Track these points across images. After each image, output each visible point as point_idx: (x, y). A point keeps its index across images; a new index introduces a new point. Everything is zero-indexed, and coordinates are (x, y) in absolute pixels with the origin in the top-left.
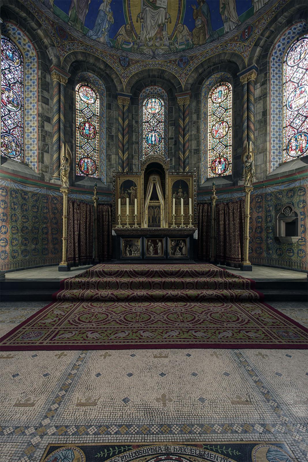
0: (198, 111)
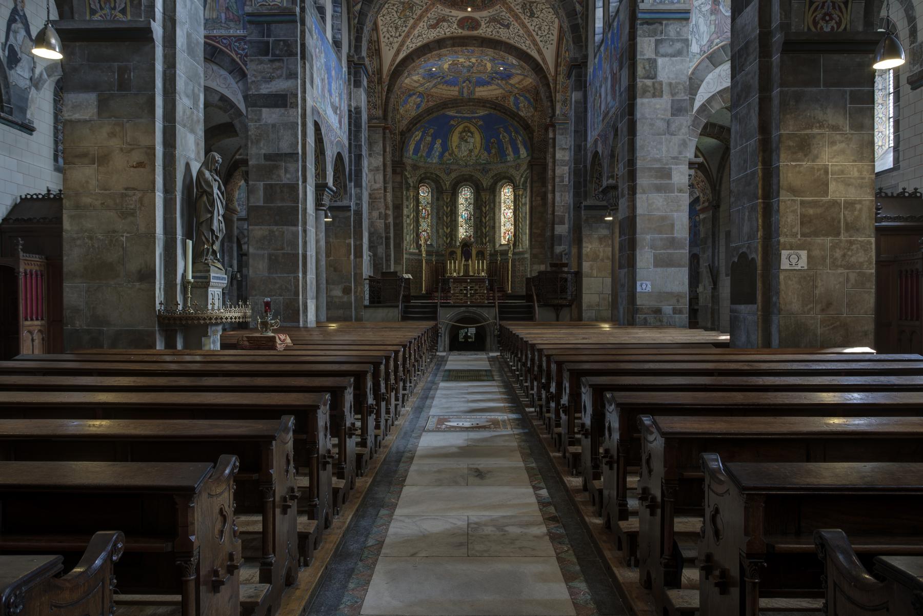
0: (494, 202)
